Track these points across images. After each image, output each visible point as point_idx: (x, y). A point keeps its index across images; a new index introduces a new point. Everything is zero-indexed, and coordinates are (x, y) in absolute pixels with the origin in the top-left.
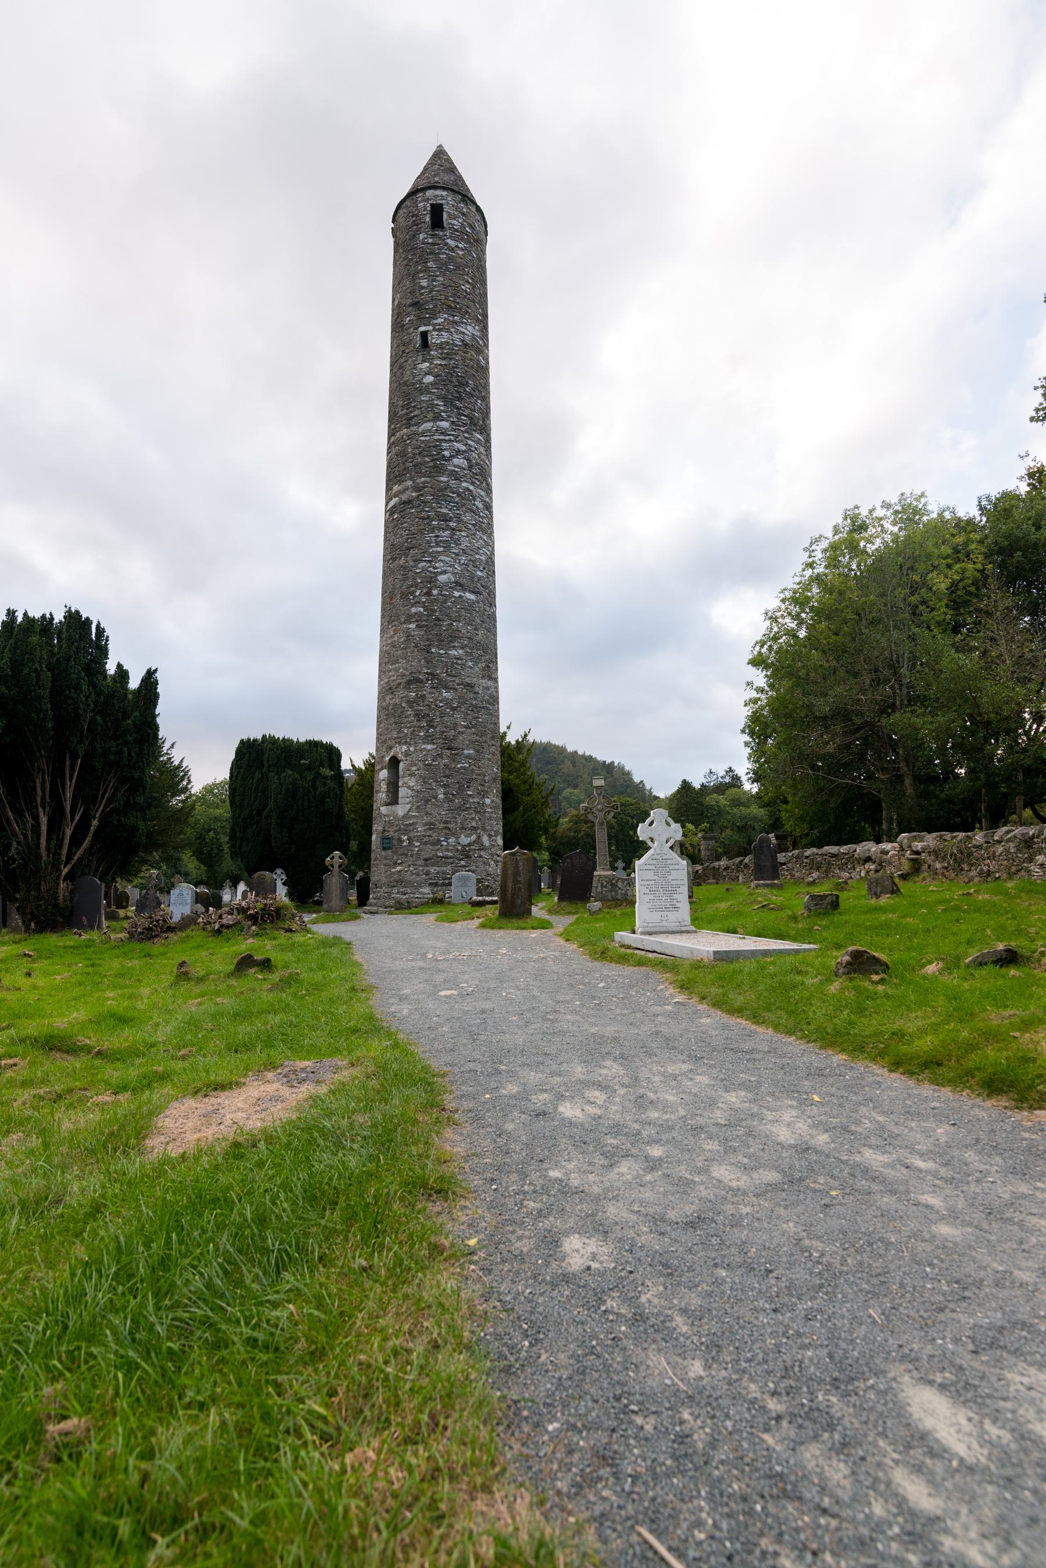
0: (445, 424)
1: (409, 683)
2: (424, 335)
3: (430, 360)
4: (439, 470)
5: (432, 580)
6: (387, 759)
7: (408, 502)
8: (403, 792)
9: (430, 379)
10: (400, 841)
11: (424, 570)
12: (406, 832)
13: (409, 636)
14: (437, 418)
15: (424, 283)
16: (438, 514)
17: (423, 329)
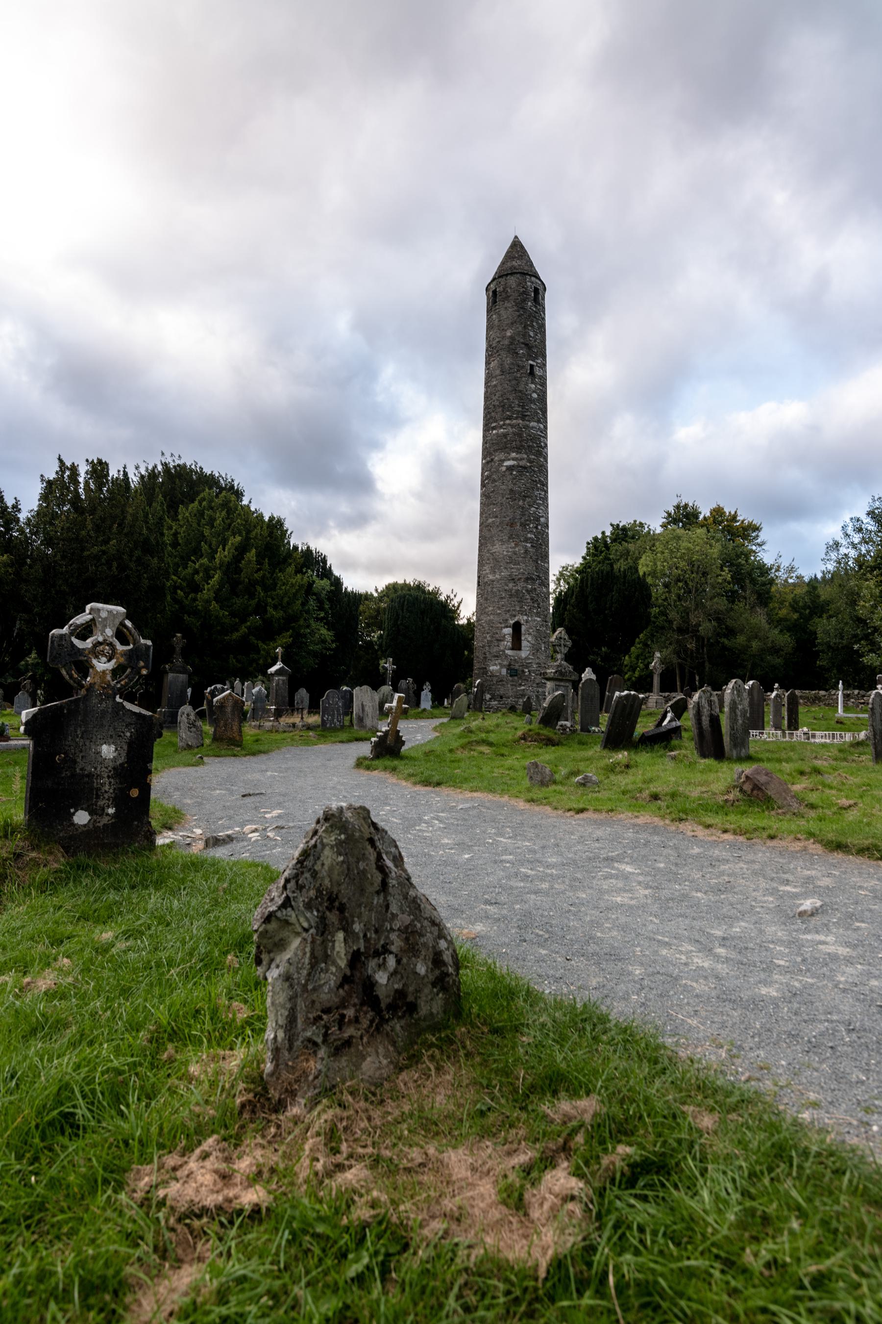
1: (527, 579)
3: (535, 384)
6: (512, 622)
7: (525, 468)
8: (524, 643)
10: (523, 672)
12: (527, 667)
13: (526, 551)
15: (532, 334)
17: (531, 362)
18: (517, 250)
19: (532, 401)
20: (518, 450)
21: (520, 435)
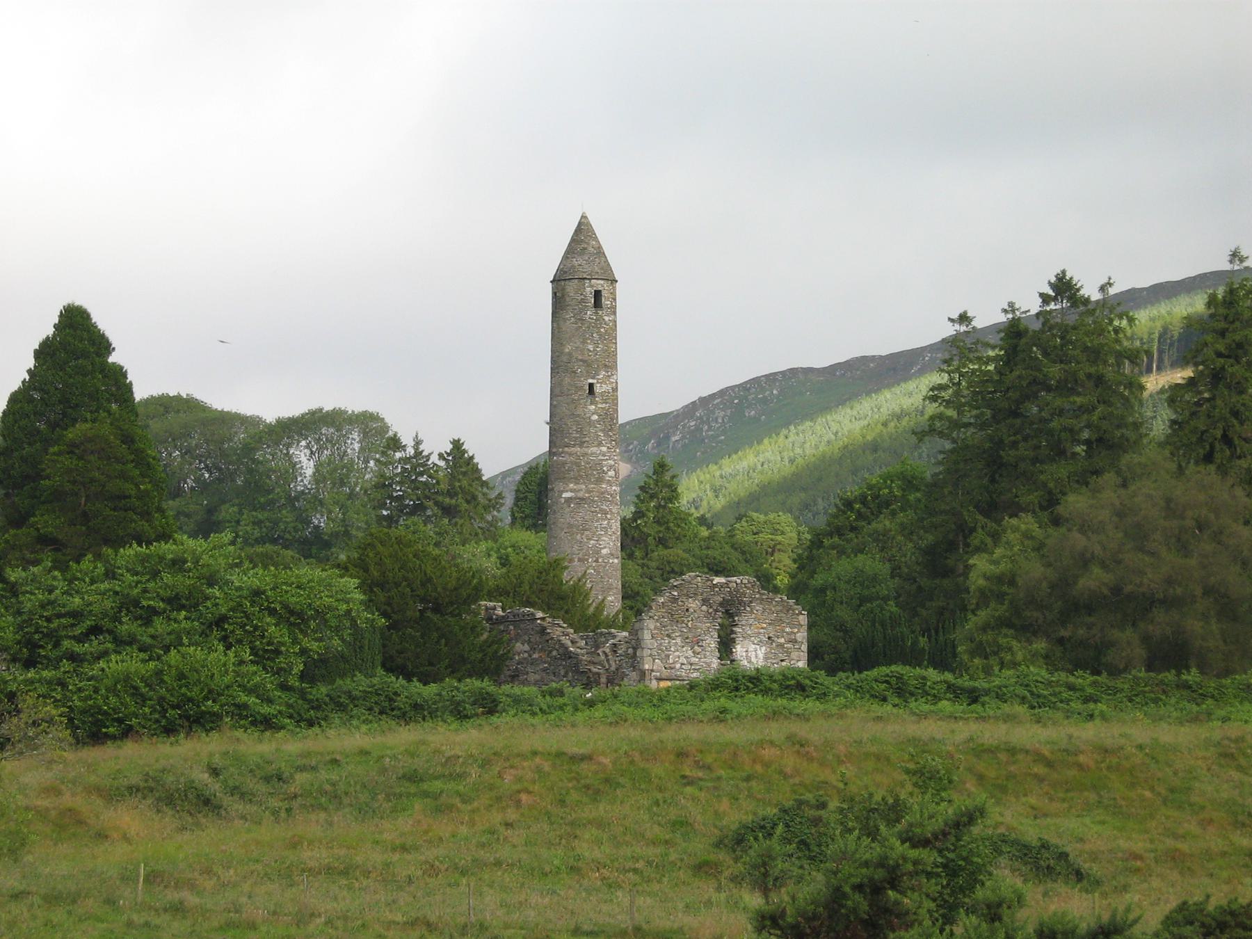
0: (604, 449)
2: (591, 385)
4: (600, 480)
5: (598, 552)
9: (595, 417)
11: (594, 546)
14: (600, 444)
15: (591, 347)
16: (601, 510)
17: (591, 381)
18: (583, 235)
19: (591, 423)
20: (576, 480)
21: (578, 465)
